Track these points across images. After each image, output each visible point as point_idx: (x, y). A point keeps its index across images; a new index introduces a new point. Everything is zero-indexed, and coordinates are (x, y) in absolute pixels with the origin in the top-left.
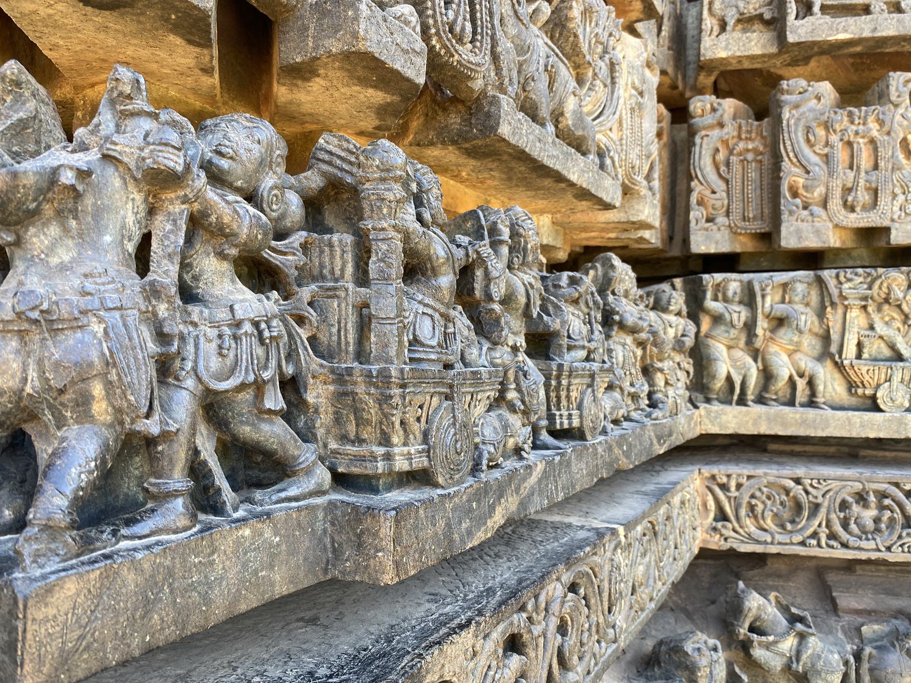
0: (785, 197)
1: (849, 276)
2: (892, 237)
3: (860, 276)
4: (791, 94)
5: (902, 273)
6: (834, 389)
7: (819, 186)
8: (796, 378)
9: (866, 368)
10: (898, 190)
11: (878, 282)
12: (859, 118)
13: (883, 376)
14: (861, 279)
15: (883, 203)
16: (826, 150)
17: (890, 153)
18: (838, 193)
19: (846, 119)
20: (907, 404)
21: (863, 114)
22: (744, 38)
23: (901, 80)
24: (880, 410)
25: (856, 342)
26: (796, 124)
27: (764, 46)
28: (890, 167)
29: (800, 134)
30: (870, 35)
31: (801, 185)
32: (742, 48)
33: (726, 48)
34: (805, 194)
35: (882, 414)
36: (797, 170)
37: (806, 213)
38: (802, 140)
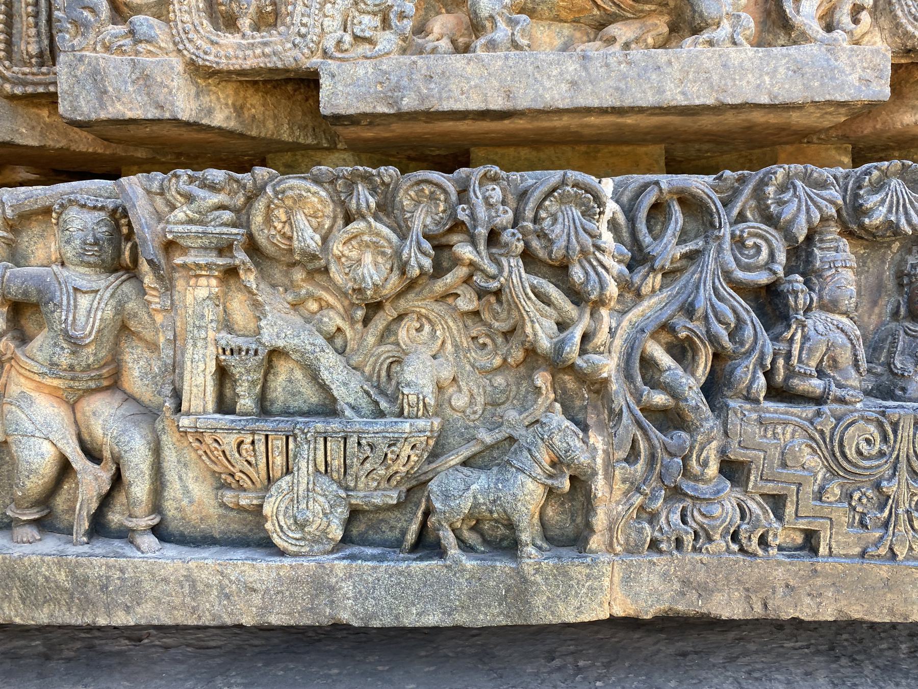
1: (184, 187)
2: (324, 94)
3: (213, 188)
5: (317, 181)
6: (186, 491)
8: (79, 461)
9: (233, 439)
11: (260, 205)
13: (278, 460)
14: (216, 199)
20: (337, 533)
24: (282, 553)
25: (212, 367)
35: (276, 561)
37: (121, 29)
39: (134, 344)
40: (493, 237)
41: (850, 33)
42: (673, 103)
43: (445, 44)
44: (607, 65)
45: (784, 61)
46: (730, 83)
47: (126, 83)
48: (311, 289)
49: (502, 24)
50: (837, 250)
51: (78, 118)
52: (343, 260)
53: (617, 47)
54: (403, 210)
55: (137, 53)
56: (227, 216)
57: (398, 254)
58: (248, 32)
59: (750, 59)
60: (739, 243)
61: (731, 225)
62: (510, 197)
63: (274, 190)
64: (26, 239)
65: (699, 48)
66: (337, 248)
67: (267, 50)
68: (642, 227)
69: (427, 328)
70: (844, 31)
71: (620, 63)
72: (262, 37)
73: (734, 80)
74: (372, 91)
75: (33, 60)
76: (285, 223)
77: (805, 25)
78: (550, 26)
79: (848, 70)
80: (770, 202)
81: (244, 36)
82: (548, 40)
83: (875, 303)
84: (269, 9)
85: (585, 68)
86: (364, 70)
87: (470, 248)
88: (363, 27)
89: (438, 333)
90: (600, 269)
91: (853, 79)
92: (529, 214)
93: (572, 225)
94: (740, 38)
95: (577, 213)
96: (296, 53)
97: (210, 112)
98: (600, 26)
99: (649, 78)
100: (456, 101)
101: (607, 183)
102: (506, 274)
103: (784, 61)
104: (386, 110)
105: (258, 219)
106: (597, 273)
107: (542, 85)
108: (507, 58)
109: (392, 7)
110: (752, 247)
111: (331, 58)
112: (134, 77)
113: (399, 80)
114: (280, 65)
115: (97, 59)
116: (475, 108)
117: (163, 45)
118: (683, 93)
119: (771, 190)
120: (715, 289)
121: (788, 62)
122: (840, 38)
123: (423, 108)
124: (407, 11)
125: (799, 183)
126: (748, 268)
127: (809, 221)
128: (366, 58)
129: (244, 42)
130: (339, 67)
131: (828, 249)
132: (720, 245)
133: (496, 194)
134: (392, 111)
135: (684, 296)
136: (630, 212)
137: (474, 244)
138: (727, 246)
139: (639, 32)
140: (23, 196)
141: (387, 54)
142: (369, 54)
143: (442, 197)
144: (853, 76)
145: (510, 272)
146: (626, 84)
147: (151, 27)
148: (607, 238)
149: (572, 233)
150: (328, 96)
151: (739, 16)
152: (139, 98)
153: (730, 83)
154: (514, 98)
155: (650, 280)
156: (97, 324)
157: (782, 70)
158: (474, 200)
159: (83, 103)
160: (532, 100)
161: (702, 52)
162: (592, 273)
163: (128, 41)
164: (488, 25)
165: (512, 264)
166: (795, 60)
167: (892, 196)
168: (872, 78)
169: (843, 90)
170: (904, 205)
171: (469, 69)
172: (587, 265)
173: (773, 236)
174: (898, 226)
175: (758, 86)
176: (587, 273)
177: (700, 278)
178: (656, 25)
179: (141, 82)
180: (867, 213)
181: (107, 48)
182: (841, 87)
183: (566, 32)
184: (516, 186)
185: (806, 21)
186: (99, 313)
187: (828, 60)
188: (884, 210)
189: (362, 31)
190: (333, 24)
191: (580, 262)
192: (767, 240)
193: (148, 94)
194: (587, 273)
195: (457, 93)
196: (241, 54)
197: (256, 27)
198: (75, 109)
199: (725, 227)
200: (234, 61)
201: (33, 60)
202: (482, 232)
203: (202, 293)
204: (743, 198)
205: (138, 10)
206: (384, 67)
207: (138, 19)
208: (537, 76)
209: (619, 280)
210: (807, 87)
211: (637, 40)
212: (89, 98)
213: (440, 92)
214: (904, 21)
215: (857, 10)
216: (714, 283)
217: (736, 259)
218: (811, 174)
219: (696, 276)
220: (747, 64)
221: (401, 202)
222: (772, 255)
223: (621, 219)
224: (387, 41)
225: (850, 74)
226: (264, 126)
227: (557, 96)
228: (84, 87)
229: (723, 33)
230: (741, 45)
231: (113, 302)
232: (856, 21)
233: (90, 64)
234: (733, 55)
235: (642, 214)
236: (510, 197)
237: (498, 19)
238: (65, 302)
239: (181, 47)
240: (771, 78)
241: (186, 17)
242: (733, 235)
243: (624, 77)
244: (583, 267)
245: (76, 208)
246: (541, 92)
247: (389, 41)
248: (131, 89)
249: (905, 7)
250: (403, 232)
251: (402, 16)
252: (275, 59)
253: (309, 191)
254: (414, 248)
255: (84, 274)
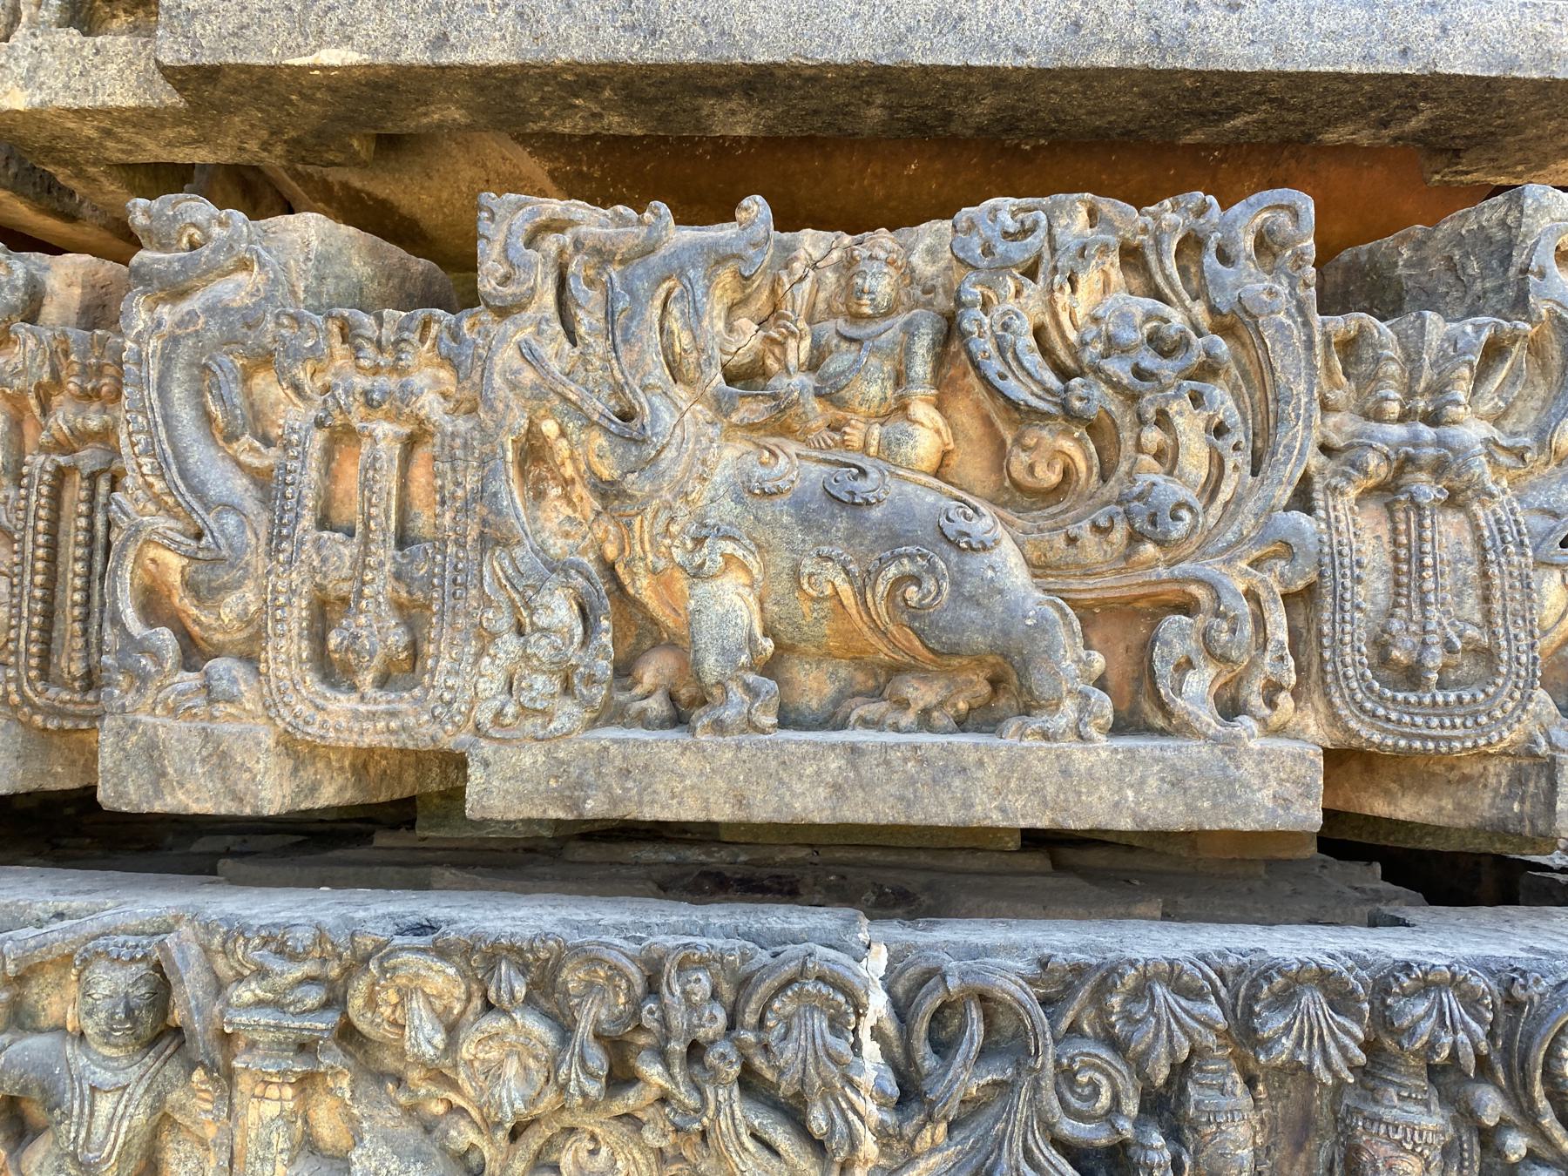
0: (116, 620)
4: (163, 247)
7: (238, 585)
10: (501, 621)
11: (360, 987)
12: (379, 345)
15: (444, 664)
16: (271, 456)
17: (471, 481)
18: (298, 613)
19: (339, 349)
21: (388, 334)
22: (88, 51)
23: (521, 223)
26: (167, 359)
27: (146, 83)
28: (473, 533)
29: (177, 393)
30: (425, 58)
31: (175, 579)
32: (77, 84)
33: (29, 80)
34: (194, 611)
36: (162, 523)
37: (191, 679)
38: (185, 415)
39: (180, 1138)
40: (695, 1051)
41: (1263, 721)
42: (987, 823)
43: (656, 706)
44: (887, 763)
45: (1156, 768)
46: (1072, 797)
47: (193, 762)
48: (433, 1089)
49: (736, 693)
50: (1222, 1089)
51: (124, 809)
52: (476, 1064)
53: (907, 719)
54: (566, 994)
55: (212, 718)
56: (314, 996)
57: (554, 1064)
58: (369, 691)
59: (1104, 763)
60: (1067, 1076)
61: (1056, 1042)
62: (725, 986)
63: (381, 964)
64: (36, 990)
65: (1026, 743)
66: (467, 1051)
67: (393, 725)
68: (923, 1049)
69: (604, 1151)
70: (1254, 717)
71: (905, 760)
72: (389, 702)
73: (1079, 793)
74: (542, 788)
75: (77, 684)
76: (396, 1006)
77: (1189, 714)
78: (819, 663)
79: (1256, 782)
80: (1114, 1018)
81: (362, 698)
82: (815, 685)
83: (1299, 1147)
84: (402, 656)
85: (855, 767)
86: (531, 758)
87: (660, 1068)
88: (534, 694)
89: (619, 1164)
90: (851, 1116)
91: (1265, 796)
92: (750, 1018)
93: (810, 1046)
94: (1092, 731)
95: (820, 1023)
96: (434, 728)
97: (314, 789)
98: (895, 670)
99: (949, 786)
100: (663, 807)
101: (879, 952)
102: (711, 1113)
103: (1156, 768)
104: (562, 815)
105: (356, 1003)
106: (847, 1121)
107: (789, 788)
108: (739, 747)
109: (577, 666)
110: (1088, 1084)
111: (486, 736)
112: (204, 753)
113: (581, 774)
114: (410, 745)
115: (155, 727)
116: (691, 818)
117: (249, 706)
118: (1003, 810)
119: (1116, 1001)
120: (1027, 1152)
121: (1161, 771)
122: (1244, 734)
123: (615, 815)
124: (599, 674)
125: (1159, 990)
126: (1079, 1116)
127: (1172, 1053)
128: (537, 739)
129: (363, 708)
130: (495, 752)
131: (1210, 1086)
132: (1037, 1080)
133: (702, 985)
134: (570, 817)
135: (980, 1157)
136: (902, 1010)
137: (667, 1066)
138: (1047, 1083)
139: (944, 693)
140: (32, 943)
141: (569, 733)
142: (541, 733)
143: (624, 985)
144: (1265, 792)
145: (718, 1111)
146: (915, 791)
147: (234, 681)
148: (871, 1049)
149: (810, 1059)
150: (477, 793)
151: (1088, 697)
152: (210, 785)
153: (1072, 797)
154: (749, 806)
155: (927, 1133)
156: (120, 1141)
157: (1153, 782)
158: (667, 998)
159: (131, 788)
160: (775, 811)
161: (1029, 749)
162: (839, 1121)
163: (200, 700)
164: (716, 691)
165: (721, 1099)
166: (1173, 768)
167: (1302, 1022)
168: (1293, 796)
169: (1246, 813)
170: (1321, 1037)
171: (683, 762)
172: (833, 1105)
173: (1119, 1071)
174: (1309, 1068)
175: (1116, 804)
176: (831, 1121)
177: (1004, 1131)
178: (971, 681)
179: (215, 760)
180: (1266, 1045)
181: (173, 712)
182: (1244, 811)
183: (843, 673)
184: (734, 971)
185: (1190, 708)
186: (125, 1123)
187: (1226, 767)
188: (1287, 1043)
189: (532, 699)
190: (490, 684)
191: (823, 1098)
192: (1109, 1076)
193: (223, 779)
194: (833, 1120)
195: (664, 796)
196: (356, 727)
197: (383, 682)
198: (120, 796)
199: (1045, 1053)
200: (346, 735)
201: (77, 684)
202: (677, 1047)
203: (271, 1109)
204: (1076, 1005)
205: (218, 651)
206: (561, 755)
207: (218, 665)
208: (785, 776)
209: (882, 1133)
210: (1191, 809)
211: (941, 705)
212: (141, 782)
213: (640, 794)
214: (1344, 712)
215: (1272, 691)
216: (1025, 1140)
217: (1062, 1100)
218: (1179, 976)
219: (1000, 1126)
220: (1100, 772)
221: (565, 983)
222: (1116, 1099)
223: (890, 1028)
224: (568, 714)
225: (1260, 790)
226: (400, 782)
227: (811, 806)
228: (134, 765)
229: (1063, 722)
230: (1091, 740)
231: (148, 1100)
232: (1271, 704)
233: (144, 733)
234: (1078, 755)
235: (921, 1027)
236: (725, 986)
237: (732, 686)
238: (76, 1111)
239: (273, 713)
240: (1137, 793)
241: (283, 671)
242: (1058, 1063)
243: (912, 781)
244: (827, 1108)
245: (104, 963)
246: (787, 798)
247: (570, 716)
248: (200, 771)
249: (1346, 692)
250: (565, 1031)
251: (590, 680)
252: (404, 736)
253: (430, 968)
254: (576, 1067)
255: (111, 1058)
